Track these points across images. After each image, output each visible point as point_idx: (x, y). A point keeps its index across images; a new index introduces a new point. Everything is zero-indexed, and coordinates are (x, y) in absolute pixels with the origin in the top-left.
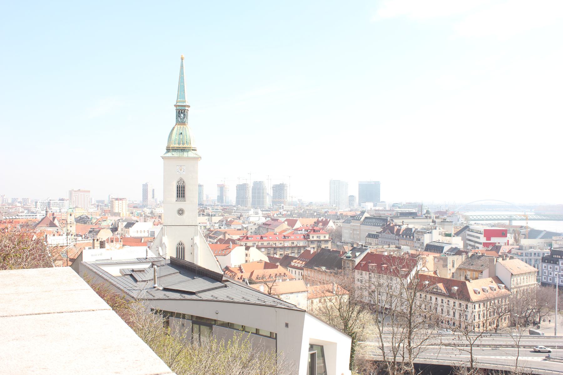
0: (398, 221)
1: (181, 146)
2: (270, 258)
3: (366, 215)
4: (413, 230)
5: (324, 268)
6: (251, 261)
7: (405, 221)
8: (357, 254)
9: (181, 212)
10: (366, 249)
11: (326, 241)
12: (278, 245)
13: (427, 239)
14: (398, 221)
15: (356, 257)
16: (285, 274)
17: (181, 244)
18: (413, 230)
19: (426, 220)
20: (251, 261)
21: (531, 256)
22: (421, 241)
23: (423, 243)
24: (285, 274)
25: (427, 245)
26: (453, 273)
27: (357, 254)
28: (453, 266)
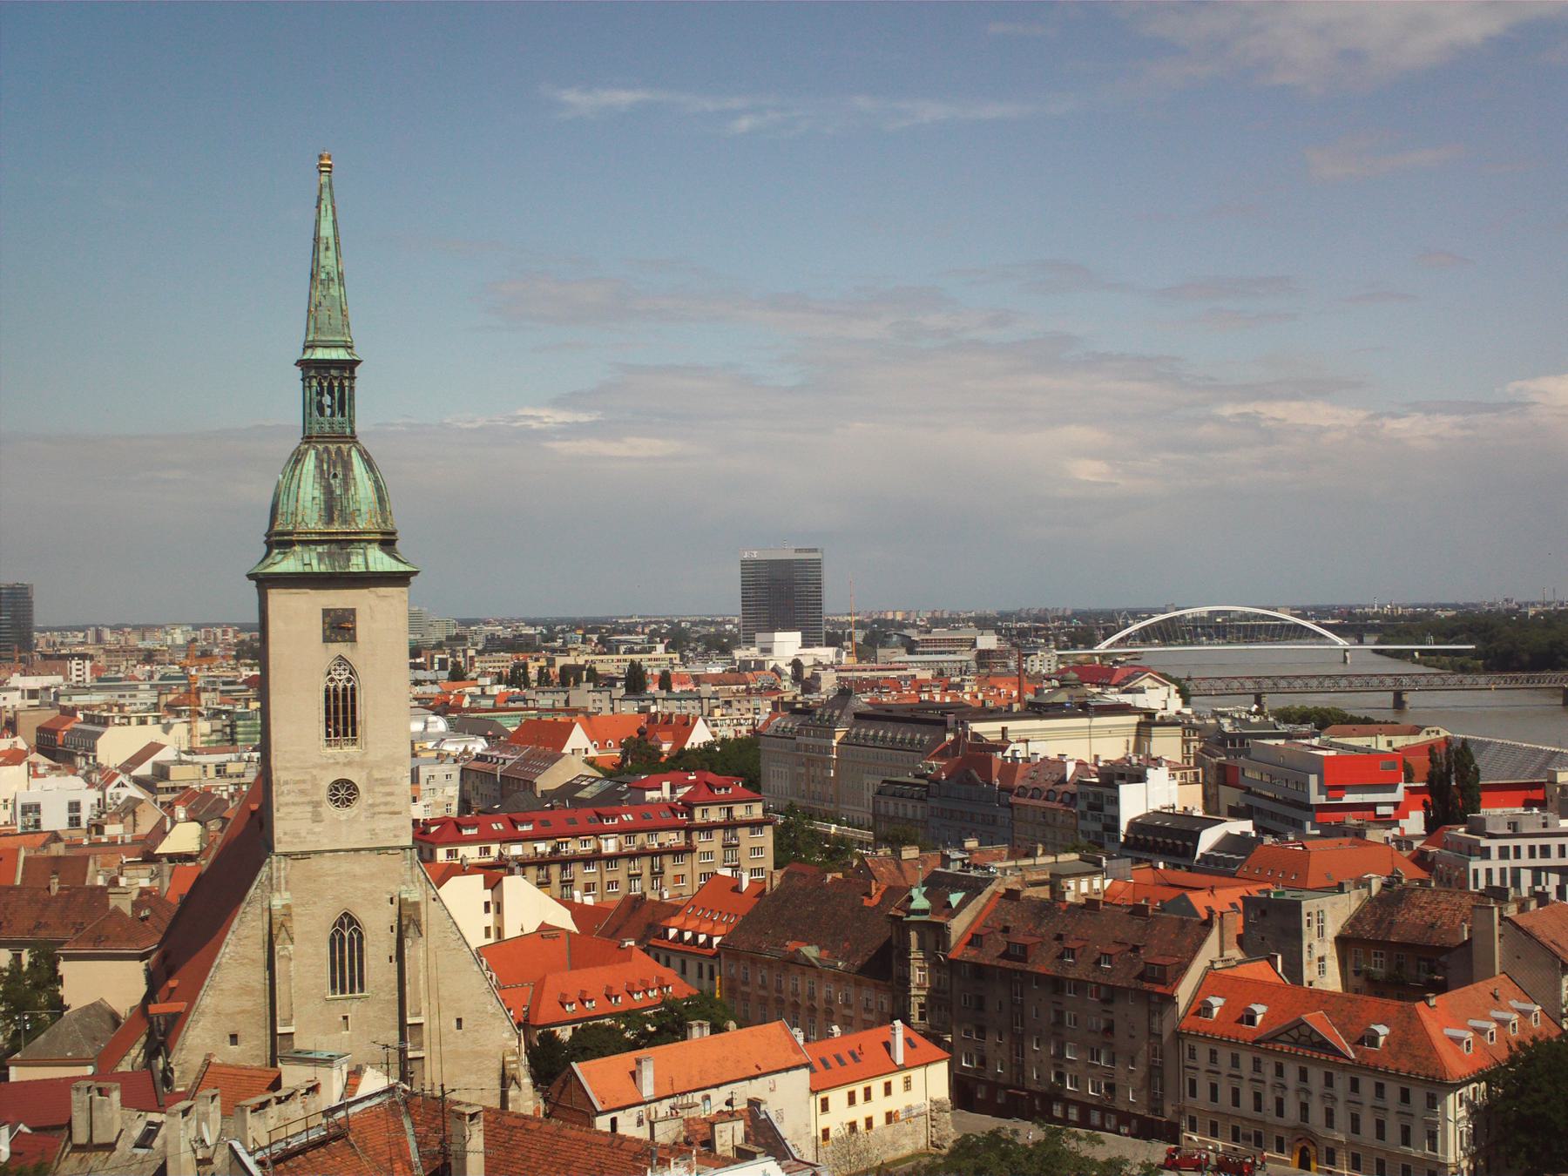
0: (988, 729)
1: (336, 527)
2: (578, 912)
3: (863, 700)
4: (1071, 769)
5: (811, 952)
6: (510, 932)
7: (1012, 725)
8: (955, 899)
9: (344, 792)
10: (988, 881)
11: (756, 825)
12: (574, 847)
13: (1133, 803)
14: (988, 729)
15: (954, 913)
16: (660, 979)
17: (347, 921)
18: (1071, 769)
19: (1084, 722)
20: (510, 932)
21: (1517, 855)
22: (1108, 810)
23: (1116, 819)
24: (660, 979)
25: (1133, 824)
26: (1321, 959)
27: (955, 899)
28: (1321, 932)
